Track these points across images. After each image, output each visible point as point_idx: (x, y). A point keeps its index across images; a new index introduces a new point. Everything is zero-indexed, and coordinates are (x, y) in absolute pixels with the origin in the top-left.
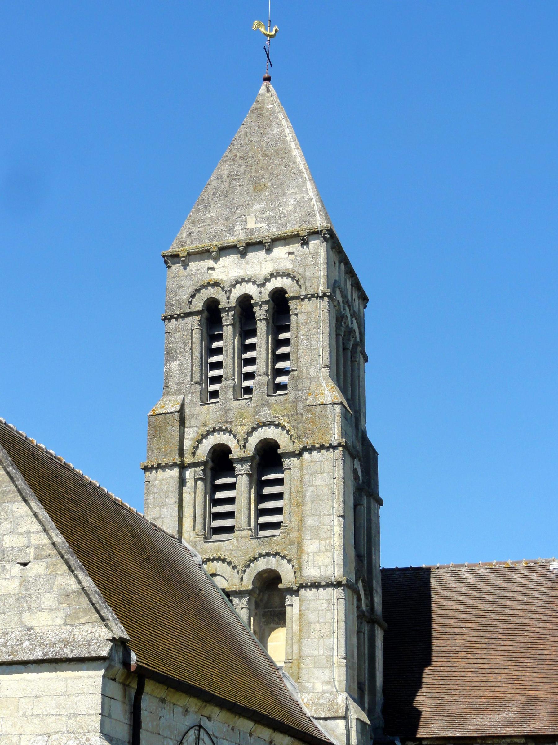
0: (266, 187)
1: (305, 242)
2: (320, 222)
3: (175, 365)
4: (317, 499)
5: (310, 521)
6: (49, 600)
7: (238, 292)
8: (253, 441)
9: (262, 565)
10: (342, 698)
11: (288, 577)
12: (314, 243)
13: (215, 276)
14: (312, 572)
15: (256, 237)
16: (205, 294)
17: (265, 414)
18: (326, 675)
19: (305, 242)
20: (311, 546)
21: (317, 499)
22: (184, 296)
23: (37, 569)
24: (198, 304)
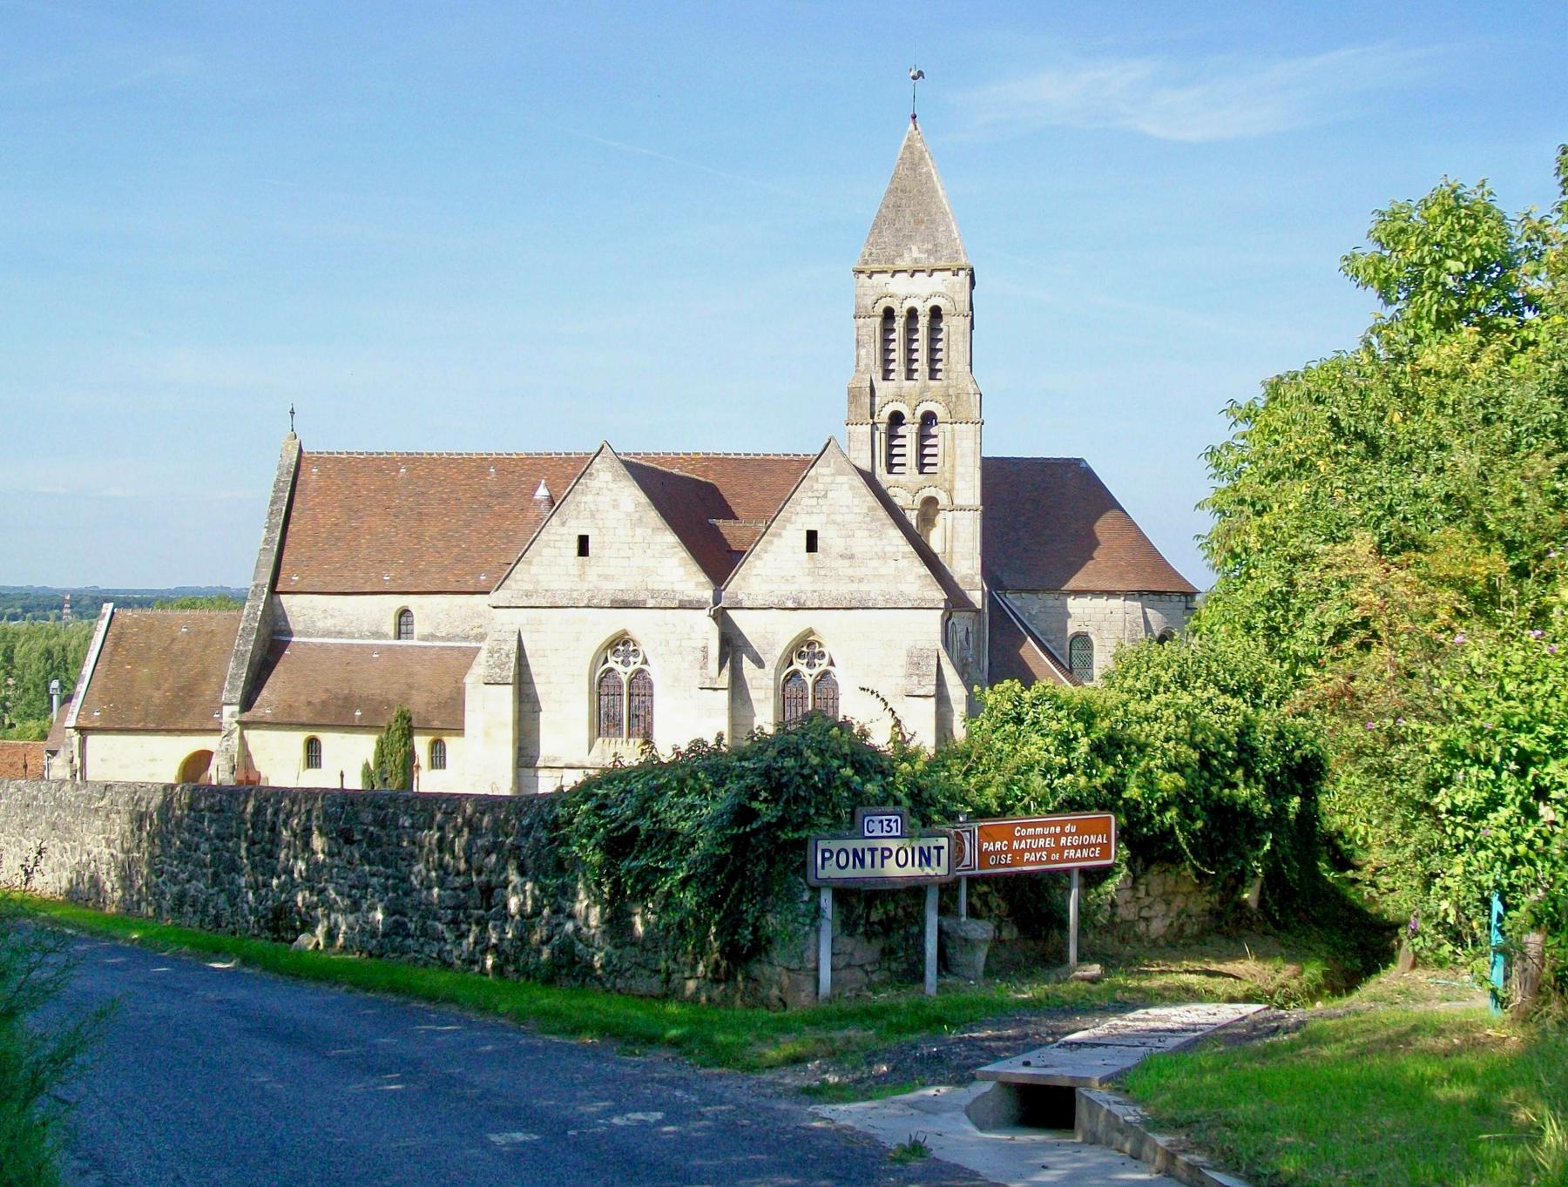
0: (922, 221)
1: (955, 274)
2: (963, 261)
3: (863, 352)
4: (963, 455)
5: (959, 470)
6: (911, 578)
7: (907, 305)
8: (919, 413)
9: (927, 493)
10: (978, 578)
11: (943, 499)
12: (962, 273)
13: (891, 289)
14: (958, 501)
15: (919, 266)
16: (883, 304)
17: (928, 395)
18: (969, 563)
19: (955, 274)
20: (958, 485)
21: (963, 455)
22: (869, 302)
23: (903, 563)
24: (880, 309)
